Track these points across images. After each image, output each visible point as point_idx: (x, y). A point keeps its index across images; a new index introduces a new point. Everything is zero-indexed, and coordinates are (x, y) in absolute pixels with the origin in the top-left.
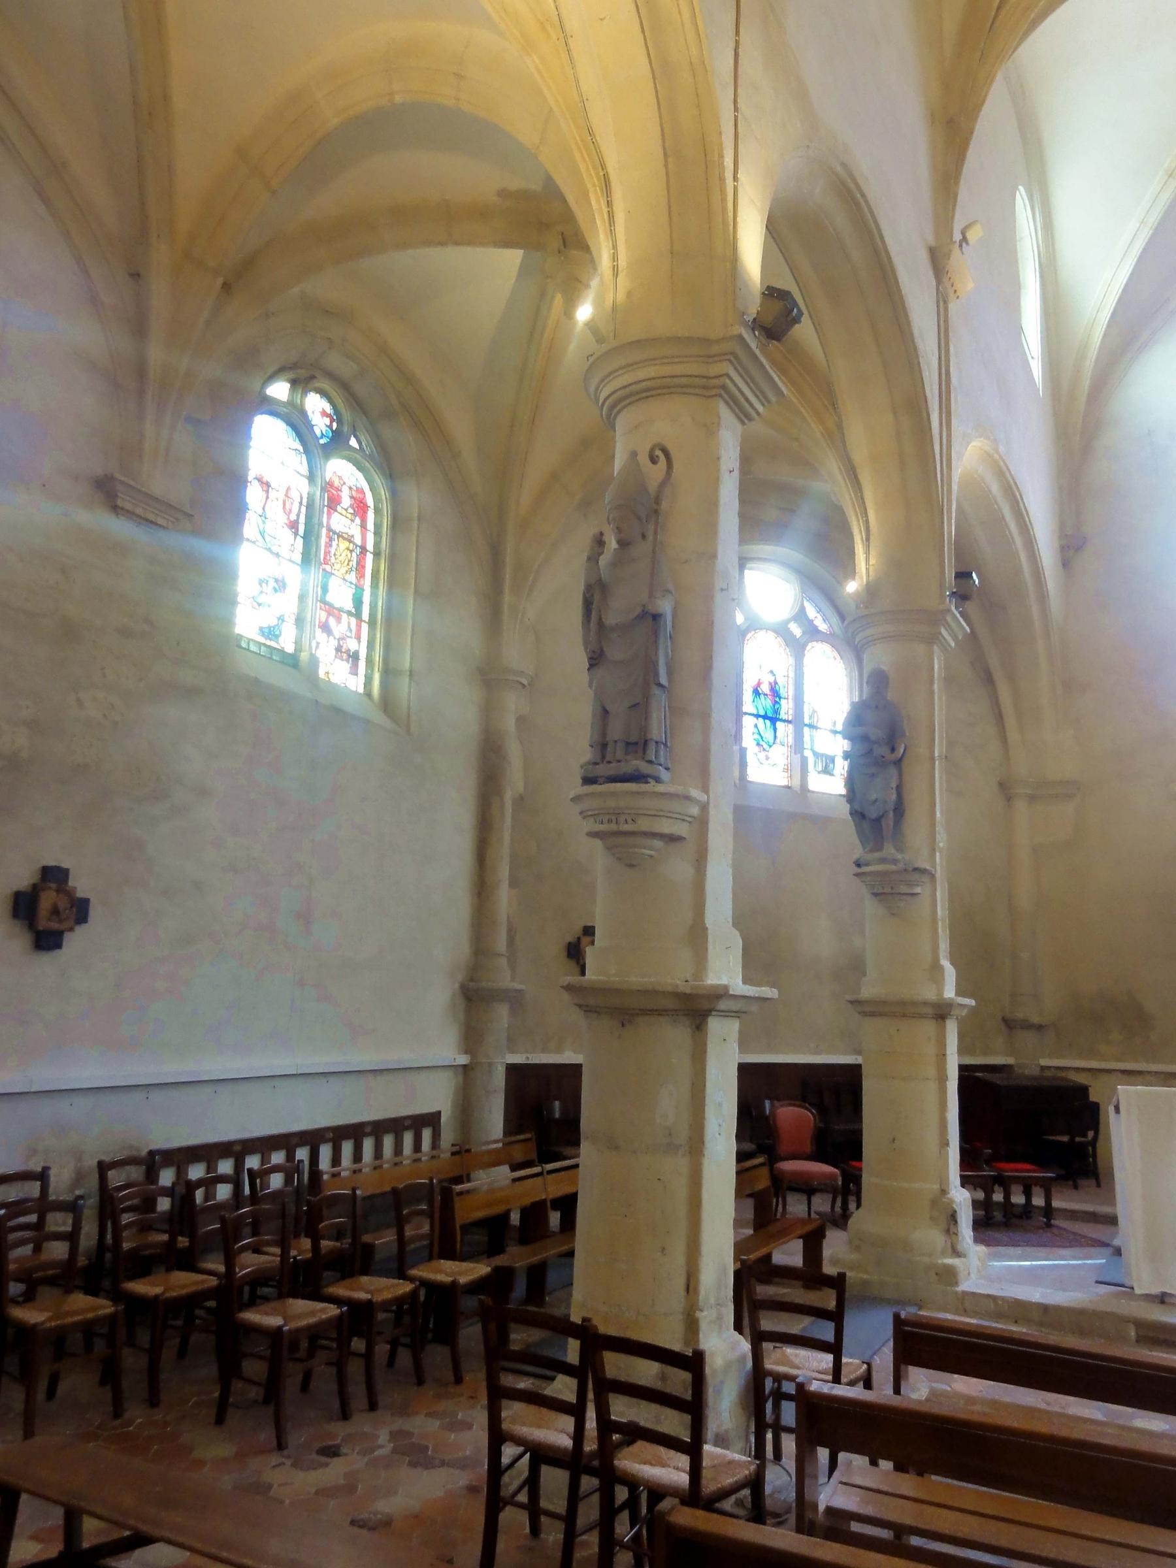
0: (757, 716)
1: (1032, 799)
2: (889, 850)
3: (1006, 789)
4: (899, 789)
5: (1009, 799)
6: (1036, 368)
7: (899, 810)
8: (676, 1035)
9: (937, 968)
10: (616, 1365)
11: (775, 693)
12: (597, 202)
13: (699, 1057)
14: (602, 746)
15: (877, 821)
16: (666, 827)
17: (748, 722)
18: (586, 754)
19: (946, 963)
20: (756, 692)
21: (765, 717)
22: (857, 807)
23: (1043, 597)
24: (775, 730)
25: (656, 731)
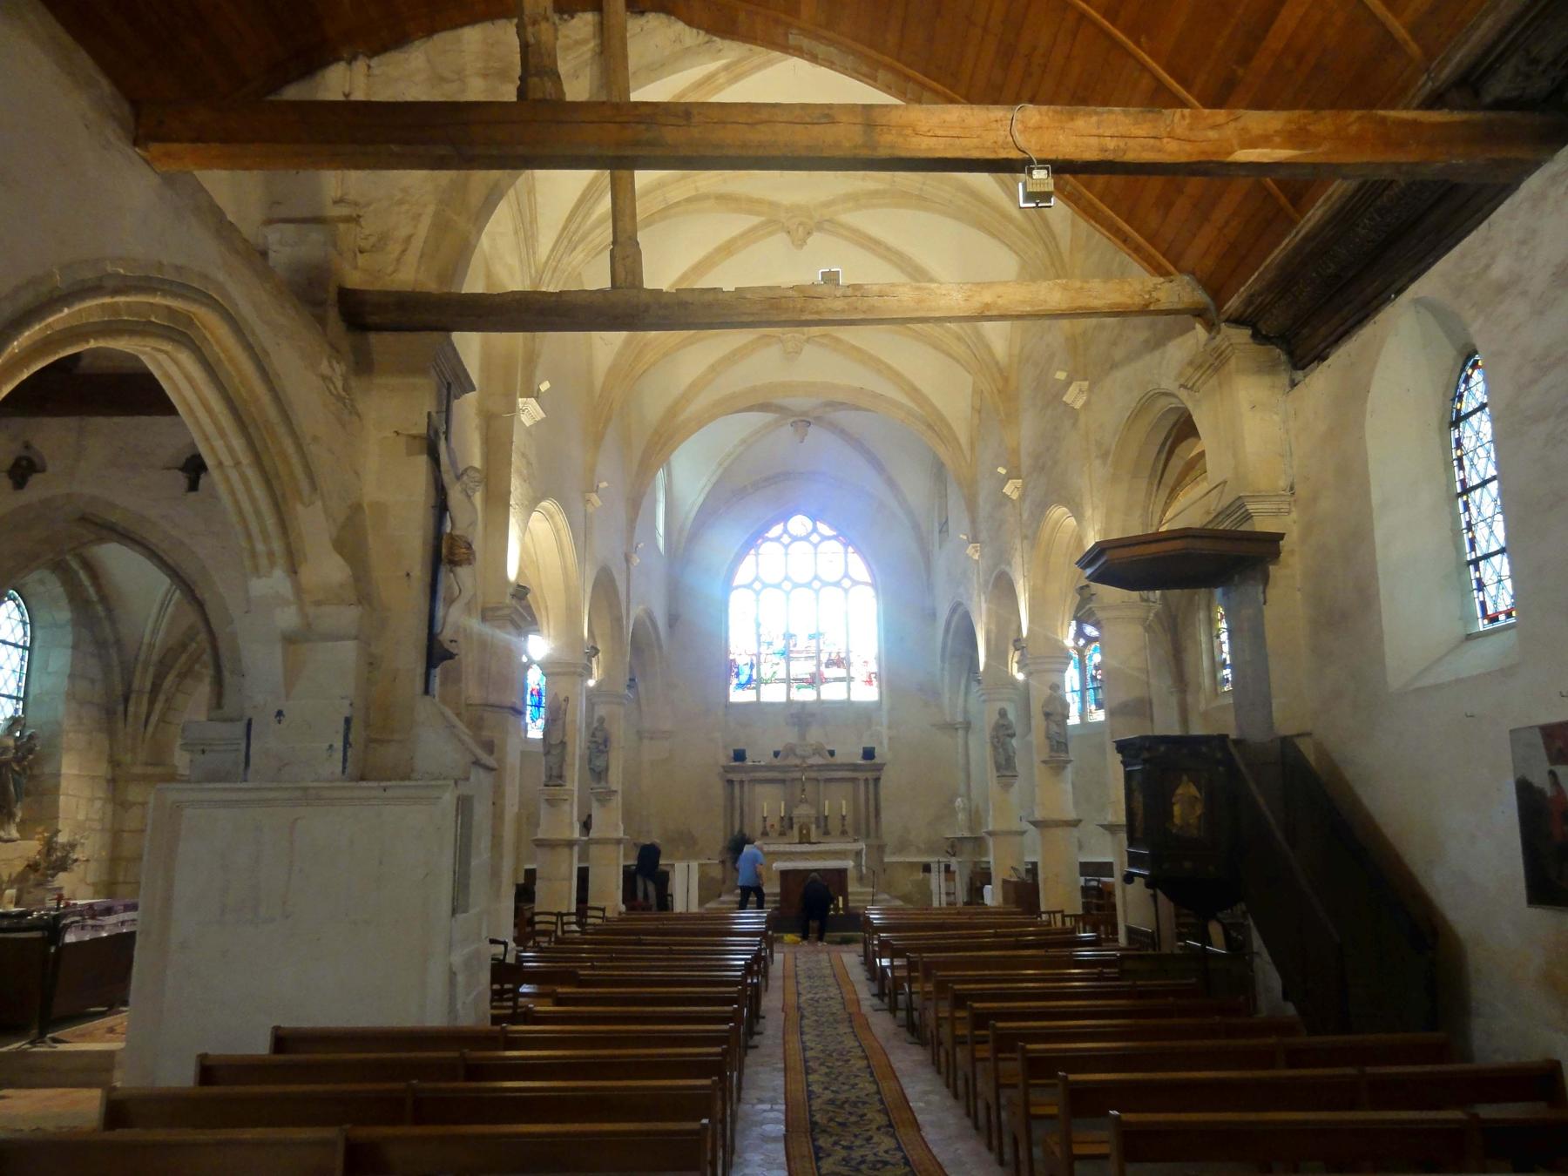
0: (532, 706)
1: (652, 738)
2: (603, 784)
3: (640, 735)
4: (607, 761)
5: (641, 739)
6: (661, 542)
7: (607, 769)
8: (566, 851)
9: (617, 825)
10: (565, 919)
11: (539, 694)
12: (544, 613)
13: (571, 855)
14: (550, 777)
15: (600, 773)
16: (566, 797)
17: (529, 708)
18: (544, 778)
19: (620, 823)
20: (532, 695)
21: (535, 706)
22: (592, 766)
23: (660, 647)
24: (539, 711)
25: (564, 773)
